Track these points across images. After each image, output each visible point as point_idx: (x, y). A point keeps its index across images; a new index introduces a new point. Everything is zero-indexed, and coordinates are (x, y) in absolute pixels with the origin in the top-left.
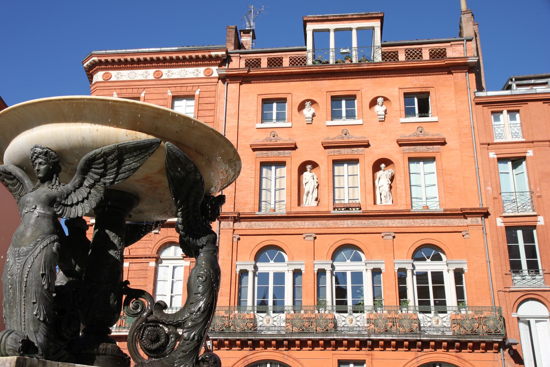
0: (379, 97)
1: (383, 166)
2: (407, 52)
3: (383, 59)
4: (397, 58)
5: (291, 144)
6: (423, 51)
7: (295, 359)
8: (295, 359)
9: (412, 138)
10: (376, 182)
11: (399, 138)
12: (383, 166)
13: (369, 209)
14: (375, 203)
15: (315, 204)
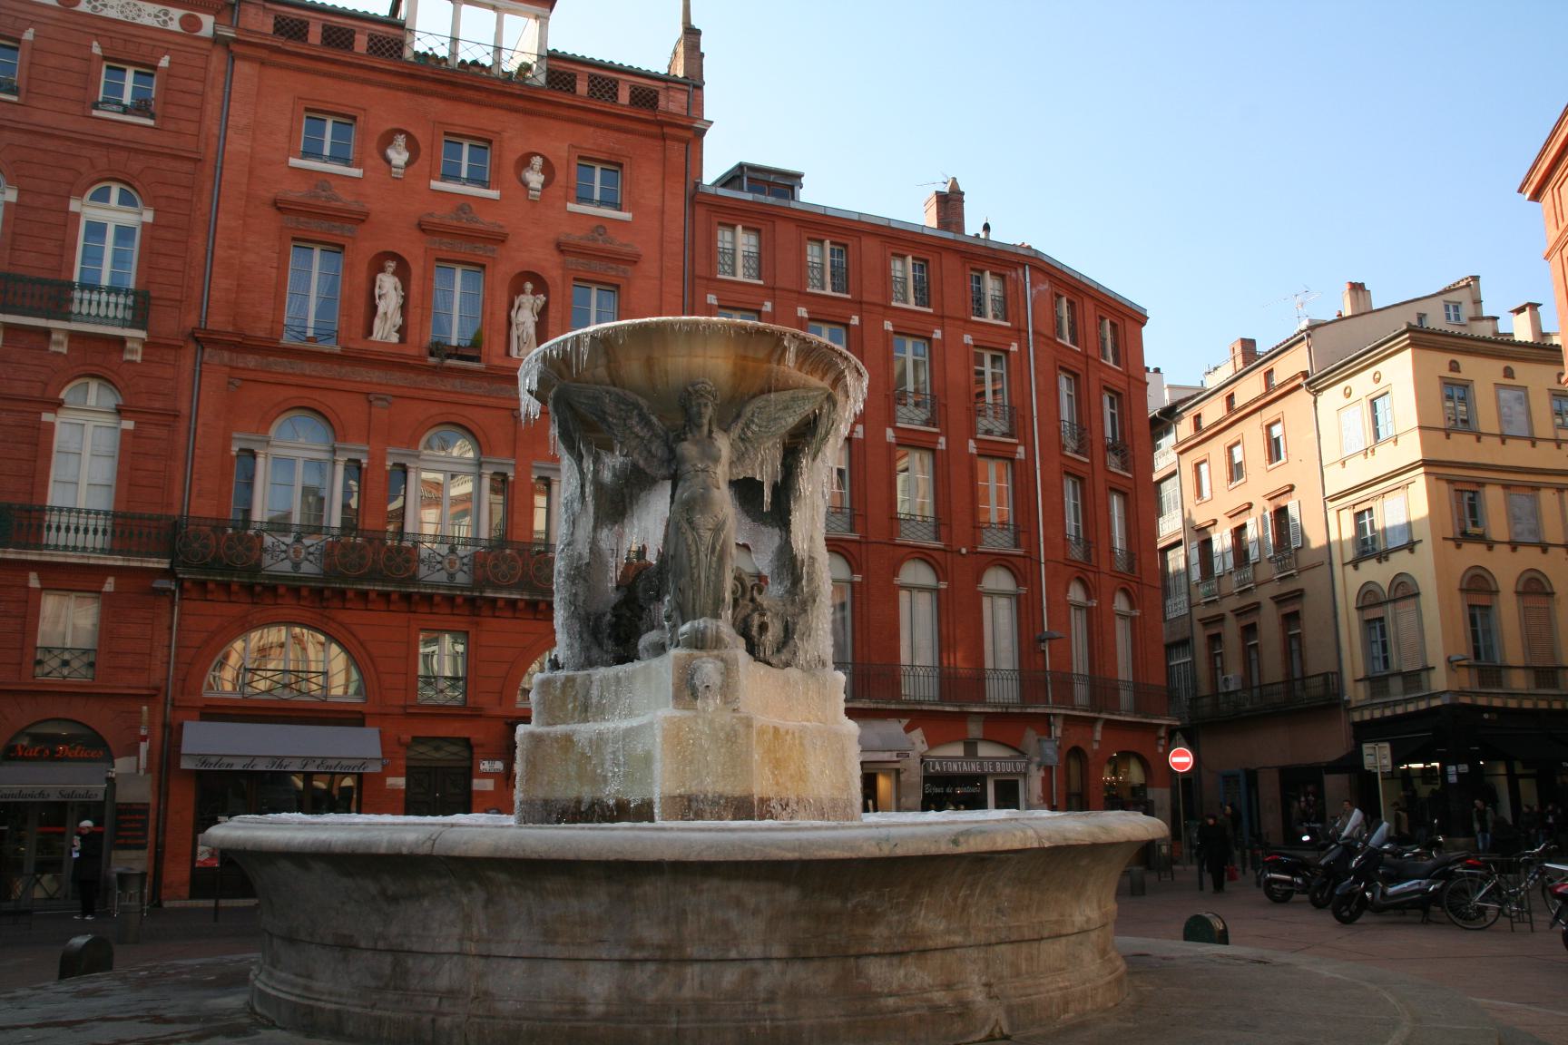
0: (536, 154)
1: (529, 286)
2: (592, 79)
3: (548, 82)
4: (574, 87)
5: (360, 213)
6: (621, 85)
7: (341, 624)
8: (341, 624)
9: (583, 242)
10: (513, 314)
11: (563, 238)
12: (529, 286)
13: (497, 362)
14: (508, 354)
15: (395, 338)
